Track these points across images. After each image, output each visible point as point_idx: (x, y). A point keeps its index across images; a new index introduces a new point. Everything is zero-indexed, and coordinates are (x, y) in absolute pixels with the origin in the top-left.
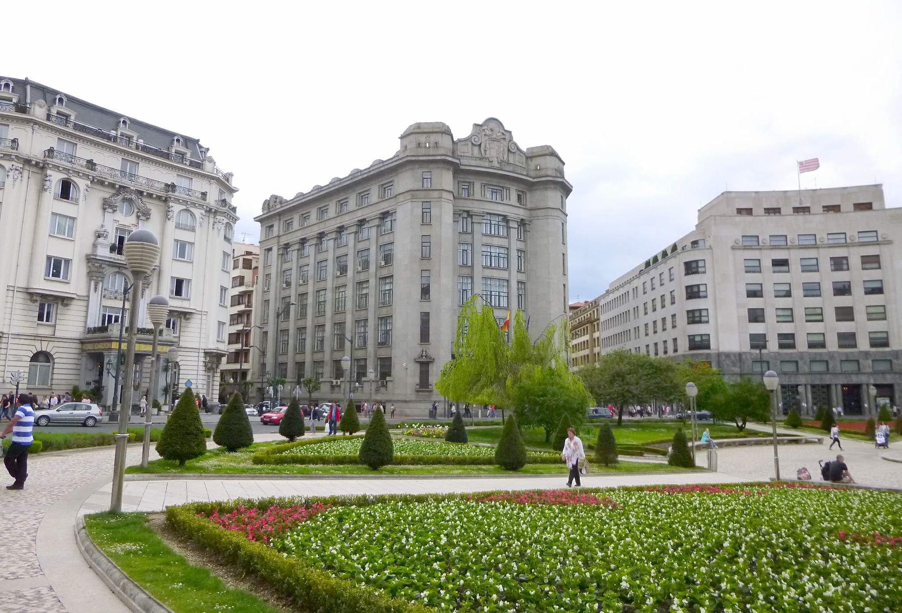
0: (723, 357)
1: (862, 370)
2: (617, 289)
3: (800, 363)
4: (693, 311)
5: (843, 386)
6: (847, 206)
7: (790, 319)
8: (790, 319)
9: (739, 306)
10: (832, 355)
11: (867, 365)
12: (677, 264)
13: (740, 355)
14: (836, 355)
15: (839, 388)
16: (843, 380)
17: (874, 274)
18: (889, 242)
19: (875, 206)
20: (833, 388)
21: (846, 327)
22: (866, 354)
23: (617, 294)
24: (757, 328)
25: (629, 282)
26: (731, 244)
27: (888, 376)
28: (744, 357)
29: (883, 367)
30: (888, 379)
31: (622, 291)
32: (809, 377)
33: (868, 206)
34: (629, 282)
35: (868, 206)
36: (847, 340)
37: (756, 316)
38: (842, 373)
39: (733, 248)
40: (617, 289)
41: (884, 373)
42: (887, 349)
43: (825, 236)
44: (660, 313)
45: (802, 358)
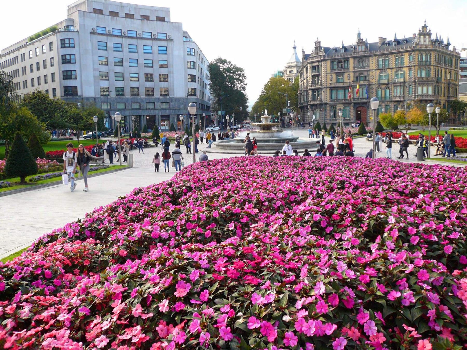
0: (85, 101)
1: (156, 108)
2: (8, 54)
3: (127, 104)
4: (67, 71)
5: (147, 116)
6: (153, 18)
7: (121, 79)
8: (121, 79)
9: (94, 70)
10: (142, 100)
11: (158, 105)
12: (55, 39)
13: (95, 99)
14: (144, 100)
15: (145, 117)
16: (146, 113)
17: (164, 57)
18: (171, 40)
19: (166, 19)
20: (142, 117)
21: (149, 84)
22: (159, 99)
23: (8, 57)
24: (105, 84)
25: (18, 49)
26: (91, 30)
27: (167, 111)
28: (97, 100)
29: (164, 106)
30: (167, 112)
31: (12, 56)
32: (131, 111)
33: (161, 19)
34: (18, 49)
35: (161, 19)
36: (150, 92)
37: (105, 76)
38: (147, 109)
39: (91, 33)
40: (8, 54)
41: (165, 109)
42: (168, 97)
43: (141, 33)
44: (43, 72)
45: (128, 101)
